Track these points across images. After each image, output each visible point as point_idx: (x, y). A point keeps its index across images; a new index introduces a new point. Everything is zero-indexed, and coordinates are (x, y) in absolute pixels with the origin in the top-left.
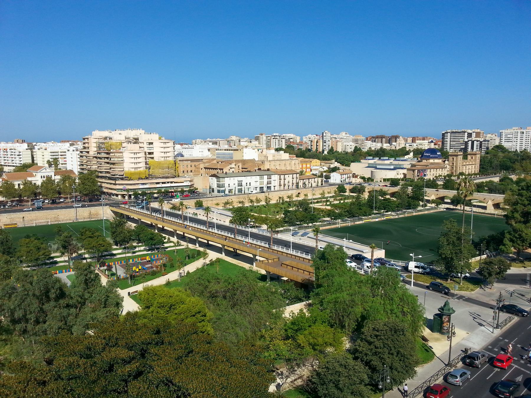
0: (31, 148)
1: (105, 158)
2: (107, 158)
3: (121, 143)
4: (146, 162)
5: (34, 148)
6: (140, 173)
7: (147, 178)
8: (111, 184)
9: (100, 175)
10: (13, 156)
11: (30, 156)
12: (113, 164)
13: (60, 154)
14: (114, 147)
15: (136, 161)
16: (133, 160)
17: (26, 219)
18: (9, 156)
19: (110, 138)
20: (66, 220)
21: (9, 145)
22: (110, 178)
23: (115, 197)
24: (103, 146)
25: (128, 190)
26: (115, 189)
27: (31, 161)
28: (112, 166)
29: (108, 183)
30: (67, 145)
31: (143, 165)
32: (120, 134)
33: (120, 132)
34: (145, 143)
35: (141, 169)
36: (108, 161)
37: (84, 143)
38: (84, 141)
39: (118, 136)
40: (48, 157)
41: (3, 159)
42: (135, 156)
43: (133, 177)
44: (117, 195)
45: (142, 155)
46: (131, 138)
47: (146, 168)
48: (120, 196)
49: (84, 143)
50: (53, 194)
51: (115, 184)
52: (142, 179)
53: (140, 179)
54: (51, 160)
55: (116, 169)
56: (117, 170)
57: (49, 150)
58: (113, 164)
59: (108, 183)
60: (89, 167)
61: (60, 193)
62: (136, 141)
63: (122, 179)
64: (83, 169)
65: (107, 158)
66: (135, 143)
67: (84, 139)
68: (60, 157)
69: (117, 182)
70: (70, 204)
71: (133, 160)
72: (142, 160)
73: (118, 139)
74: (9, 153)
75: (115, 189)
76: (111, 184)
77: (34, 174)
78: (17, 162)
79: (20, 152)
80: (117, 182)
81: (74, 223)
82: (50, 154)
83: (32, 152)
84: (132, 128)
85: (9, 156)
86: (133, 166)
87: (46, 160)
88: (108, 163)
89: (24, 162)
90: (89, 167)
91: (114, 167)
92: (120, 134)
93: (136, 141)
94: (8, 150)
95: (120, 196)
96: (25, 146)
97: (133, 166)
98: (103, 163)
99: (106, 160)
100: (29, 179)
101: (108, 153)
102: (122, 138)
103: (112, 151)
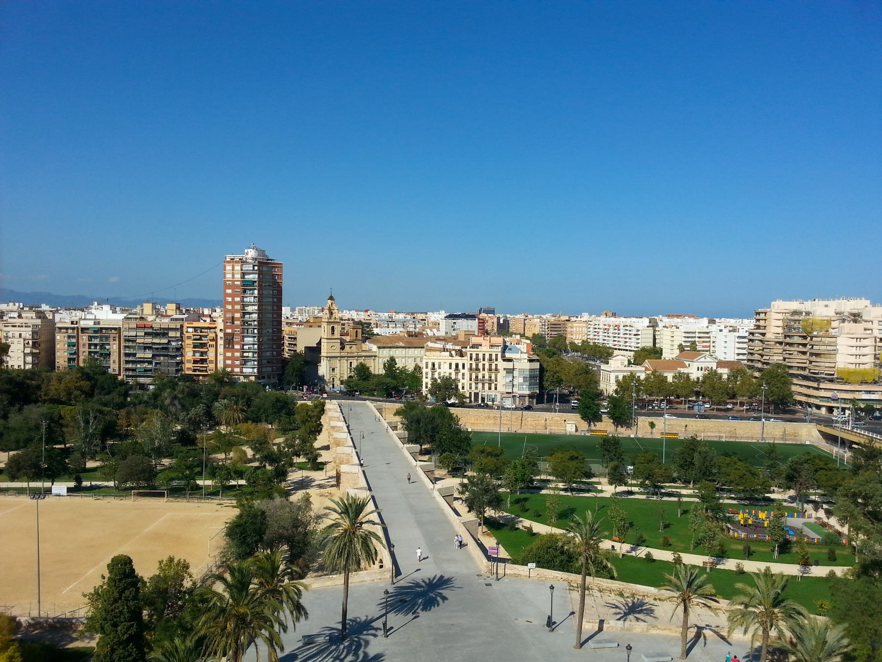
0: (653, 325)
1: (799, 344)
2: (805, 345)
3: (829, 322)
4: (875, 355)
5: (657, 325)
6: (864, 373)
7: (875, 382)
8: (809, 387)
9: (791, 371)
10: (627, 336)
11: (652, 336)
12: (817, 355)
13: (697, 335)
14: (817, 327)
15: (858, 352)
16: (853, 351)
17: (689, 428)
18: (621, 335)
19: (808, 313)
20: (748, 438)
21: (628, 321)
22: (805, 378)
23: (814, 410)
24: (796, 326)
25: (836, 400)
26: (816, 397)
27: (651, 344)
28: (814, 358)
29: (801, 386)
30: (705, 321)
31: (870, 359)
32: (826, 306)
33: (826, 303)
34: (876, 323)
35: (867, 367)
36: (804, 350)
37: (758, 320)
38: (758, 317)
39: (821, 309)
40: (680, 339)
41: (612, 339)
42: (858, 344)
43: (852, 379)
44: (818, 407)
45: (870, 342)
46: (846, 314)
47: (876, 365)
48: (823, 410)
49: (758, 320)
50: (716, 394)
51: (817, 389)
52: (866, 383)
53: (863, 382)
54: (684, 344)
55: (822, 364)
56: (822, 366)
57: (683, 329)
58: (817, 355)
59: (801, 386)
60: (767, 358)
61: (733, 396)
62: (856, 317)
63: (831, 381)
64: (752, 361)
65: (805, 345)
66: (855, 321)
67: (759, 313)
68: (697, 339)
69: (822, 386)
70: (744, 414)
71: (853, 351)
72: (870, 351)
73: (824, 314)
74: (622, 332)
75: (816, 397)
76: (809, 387)
77: (687, 363)
78: (633, 344)
79: (638, 331)
80: (822, 386)
81: (758, 443)
82: (684, 335)
83: (655, 331)
84: (848, 296)
85: (621, 335)
86: (853, 359)
87: (677, 343)
88: (804, 353)
89: (643, 345)
90: (767, 358)
91: (818, 359)
92: (826, 306)
93: (856, 317)
94: (621, 327)
95: (823, 410)
96: (646, 322)
97: (853, 359)
98: (795, 353)
99: (801, 349)
100: (682, 370)
101: (805, 338)
102: (830, 312)
103: (815, 333)
